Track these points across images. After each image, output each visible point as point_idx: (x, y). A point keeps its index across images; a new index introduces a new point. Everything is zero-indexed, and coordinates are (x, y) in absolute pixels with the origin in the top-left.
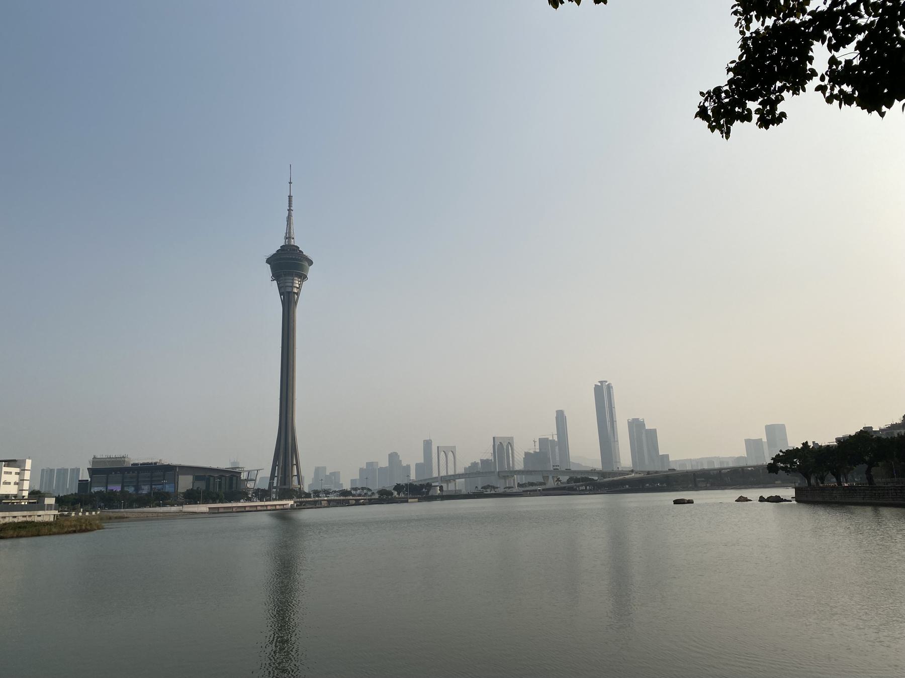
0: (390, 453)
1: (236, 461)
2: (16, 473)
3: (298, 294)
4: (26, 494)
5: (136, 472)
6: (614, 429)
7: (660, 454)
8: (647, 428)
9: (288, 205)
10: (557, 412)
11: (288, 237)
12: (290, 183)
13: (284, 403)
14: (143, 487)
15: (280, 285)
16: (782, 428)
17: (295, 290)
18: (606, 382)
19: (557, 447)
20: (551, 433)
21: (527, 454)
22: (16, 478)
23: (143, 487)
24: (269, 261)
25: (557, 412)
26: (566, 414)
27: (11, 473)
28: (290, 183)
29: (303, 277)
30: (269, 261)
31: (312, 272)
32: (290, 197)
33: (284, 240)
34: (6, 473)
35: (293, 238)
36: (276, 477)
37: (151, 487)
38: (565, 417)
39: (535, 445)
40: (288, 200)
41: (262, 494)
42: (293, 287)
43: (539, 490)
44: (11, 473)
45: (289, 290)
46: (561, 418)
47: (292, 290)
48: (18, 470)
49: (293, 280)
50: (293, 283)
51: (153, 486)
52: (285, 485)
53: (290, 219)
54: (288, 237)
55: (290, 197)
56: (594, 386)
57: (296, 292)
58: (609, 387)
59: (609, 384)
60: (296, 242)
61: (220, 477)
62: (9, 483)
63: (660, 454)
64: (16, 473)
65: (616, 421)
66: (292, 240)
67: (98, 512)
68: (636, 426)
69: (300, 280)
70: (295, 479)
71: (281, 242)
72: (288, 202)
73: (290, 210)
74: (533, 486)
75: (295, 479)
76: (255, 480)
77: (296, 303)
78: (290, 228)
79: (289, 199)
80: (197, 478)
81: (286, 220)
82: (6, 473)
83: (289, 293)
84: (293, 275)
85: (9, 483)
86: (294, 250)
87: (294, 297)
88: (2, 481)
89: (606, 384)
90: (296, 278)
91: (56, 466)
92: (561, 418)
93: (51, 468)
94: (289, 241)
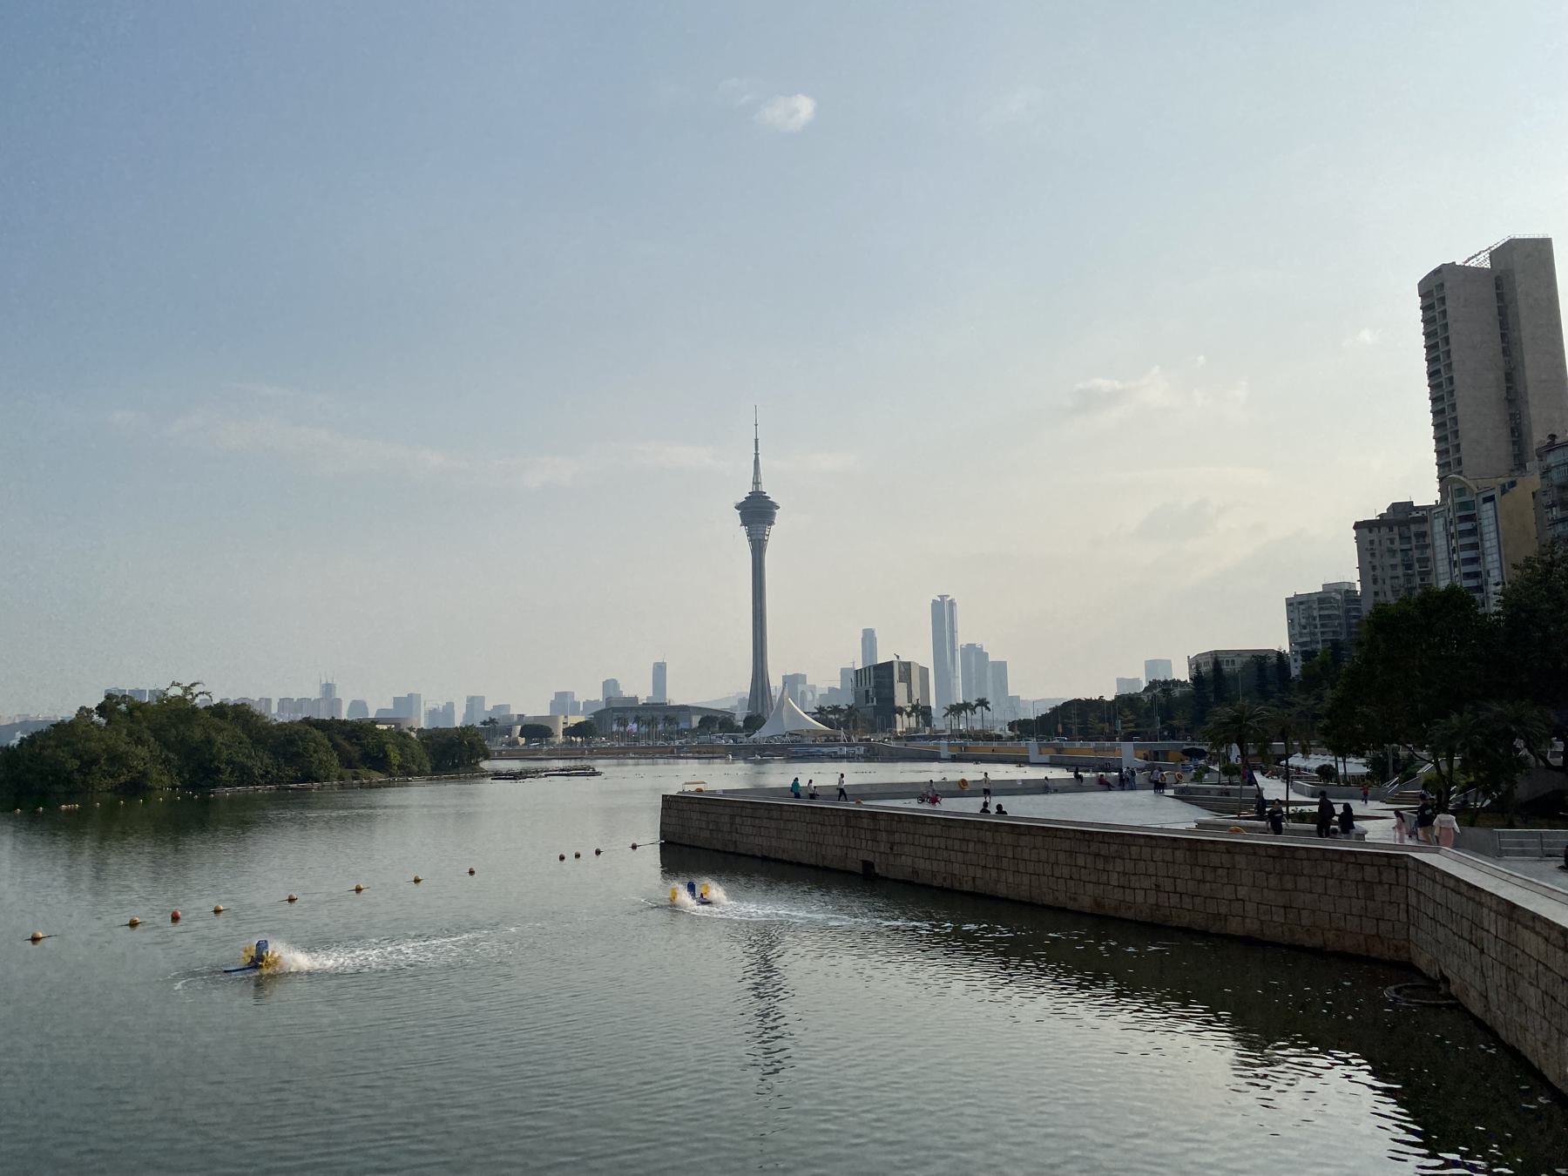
1: (330, 682)
8: (991, 659)
10: (865, 631)
11: (756, 483)
12: (756, 425)
18: (948, 596)
24: (737, 508)
25: (865, 631)
26: (877, 634)
28: (756, 425)
29: (771, 523)
32: (756, 440)
40: (754, 443)
54: (756, 483)
55: (756, 440)
56: (931, 602)
58: (952, 603)
59: (951, 600)
60: (764, 488)
63: (1010, 695)
71: (749, 488)
73: (757, 454)
94: (757, 488)
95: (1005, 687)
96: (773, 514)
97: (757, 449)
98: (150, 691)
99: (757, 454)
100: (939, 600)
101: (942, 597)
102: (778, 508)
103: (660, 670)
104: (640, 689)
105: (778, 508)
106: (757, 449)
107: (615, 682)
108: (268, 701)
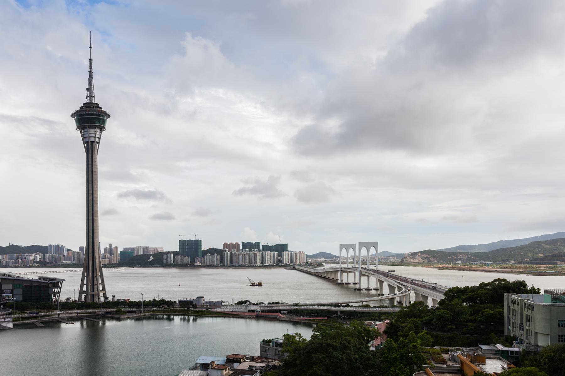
3: (98, 143)
11: (91, 96)
12: (90, 48)
17: (97, 140)
29: (102, 129)
30: (73, 116)
31: (109, 123)
35: (94, 97)
45: (92, 139)
54: (91, 96)
55: (91, 60)
60: (96, 100)
71: (86, 100)
73: (91, 72)
81: (87, 81)
83: (92, 142)
84: (96, 127)
96: (104, 122)
97: (91, 68)
99: (91, 72)
102: (109, 116)
105: (109, 116)
106: (91, 68)
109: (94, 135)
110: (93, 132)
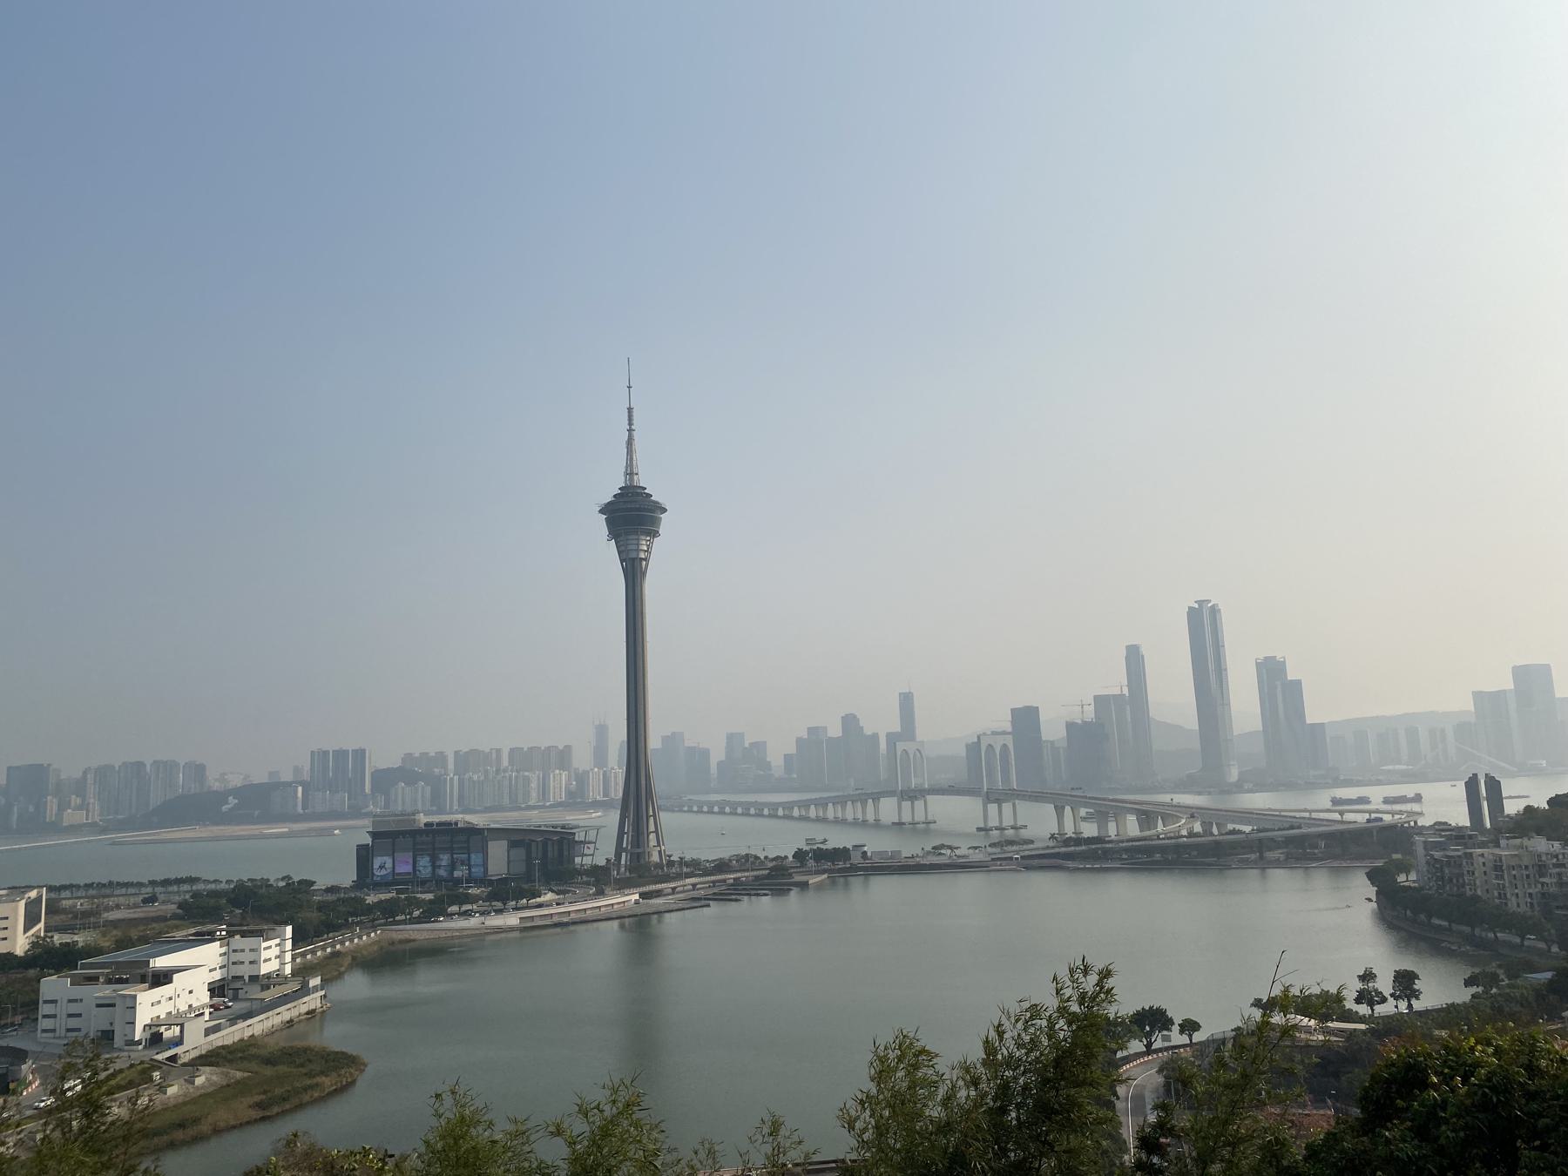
0: (843, 715)
1: (602, 723)
2: (276, 946)
4: (288, 970)
5: (431, 835)
6: (1221, 682)
7: (1309, 721)
9: (627, 422)
11: (630, 472)
12: (629, 387)
13: (633, 726)
14: (441, 856)
15: (623, 548)
16: (1545, 670)
17: (642, 555)
18: (1209, 601)
19: (1128, 708)
20: (1115, 682)
21: (1070, 726)
22: (276, 951)
23: (441, 856)
24: (601, 511)
26: (1144, 651)
27: (270, 947)
29: (655, 534)
30: (601, 511)
31: (666, 522)
32: (630, 410)
33: (623, 478)
34: (265, 949)
35: (637, 474)
36: (626, 833)
37: (452, 857)
38: (1143, 656)
39: (1083, 712)
40: (627, 414)
41: (600, 879)
42: (638, 550)
43: (1017, 859)
44: (270, 947)
45: (633, 555)
46: (1134, 658)
47: (638, 555)
48: (277, 941)
49: (638, 539)
50: (638, 545)
51: (455, 856)
52: (638, 848)
53: (631, 445)
54: (630, 472)
55: (630, 410)
57: (643, 557)
58: (1214, 611)
59: (1214, 605)
60: (642, 480)
61: (545, 843)
62: (270, 959)
64: (276, 946)
65: (1226, 670)
66: (636, 477)
67: (378, 932)
68: (1271, 673)
69: (648, 538)
70: (652, 836)
72: (627, 418)
73: (630, 430)
74: (1013, 845)
75: (652, 836)
76: (595, 843)
77: (644, 574)
78: (632, 459)
79: (629, 412)
80: (513, 844)
82: (265, 949)
83: (633, 560)
85: (270, 959)
86: (638, 494)
87: (642, 568)
88: (262, 959)
89: (1209, 605)
90: (643, 537)
91: (331, 746)
92: (1134, 658)
93: (324, 749)
94: (631, 480)
95: (1300, 713)
96: (656, 522)
97: (630, 424)
98: (333, 751)
100: (1196, 606)
101: (1200, 603)
102: (665, 510)
103: (906, 701)
104: (881, 721)
105: (665, 510)
106: (630, 424)
107: (854, 716)
108: (441, 757)
109: (634, 547)
110: (635, 542)
